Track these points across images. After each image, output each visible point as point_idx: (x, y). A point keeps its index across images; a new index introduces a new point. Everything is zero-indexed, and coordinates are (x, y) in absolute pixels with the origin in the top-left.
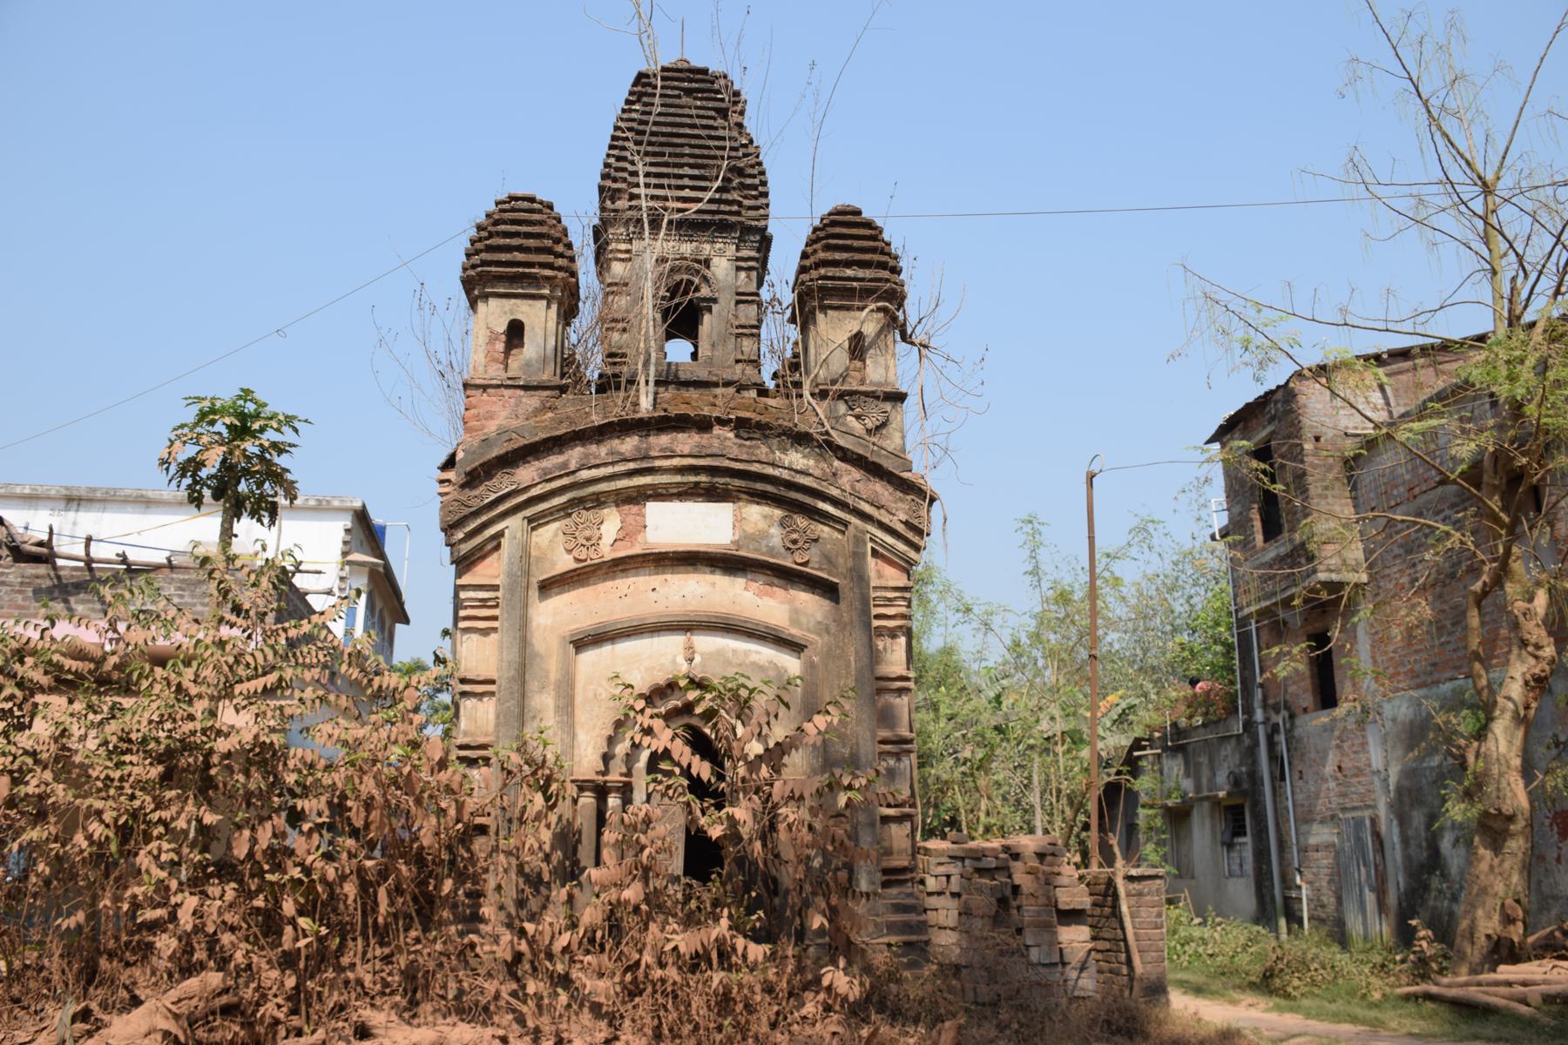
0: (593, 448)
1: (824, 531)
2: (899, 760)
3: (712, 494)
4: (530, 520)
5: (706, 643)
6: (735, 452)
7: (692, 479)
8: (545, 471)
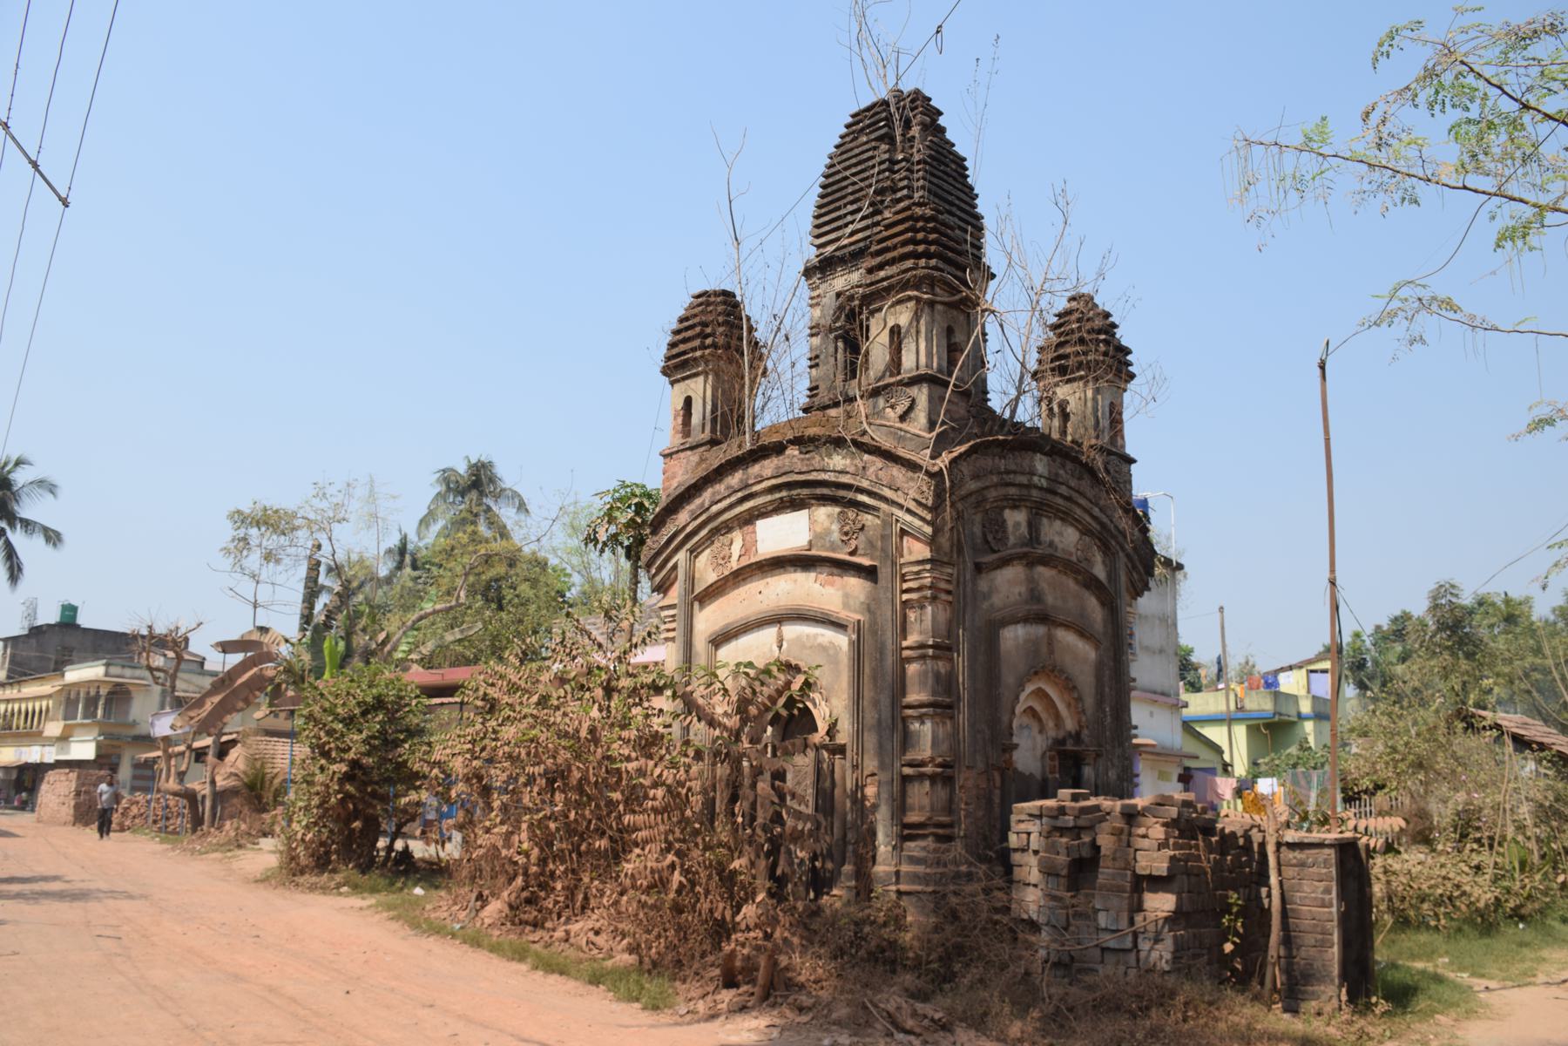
0: (717, 487)
1: (868, 519)
2: (923, 723)
3: (795, 505)
4: (691, 551)
5: (792, 631)
6: (799, 466)
7: (778, 495)
8: (692, 512)
